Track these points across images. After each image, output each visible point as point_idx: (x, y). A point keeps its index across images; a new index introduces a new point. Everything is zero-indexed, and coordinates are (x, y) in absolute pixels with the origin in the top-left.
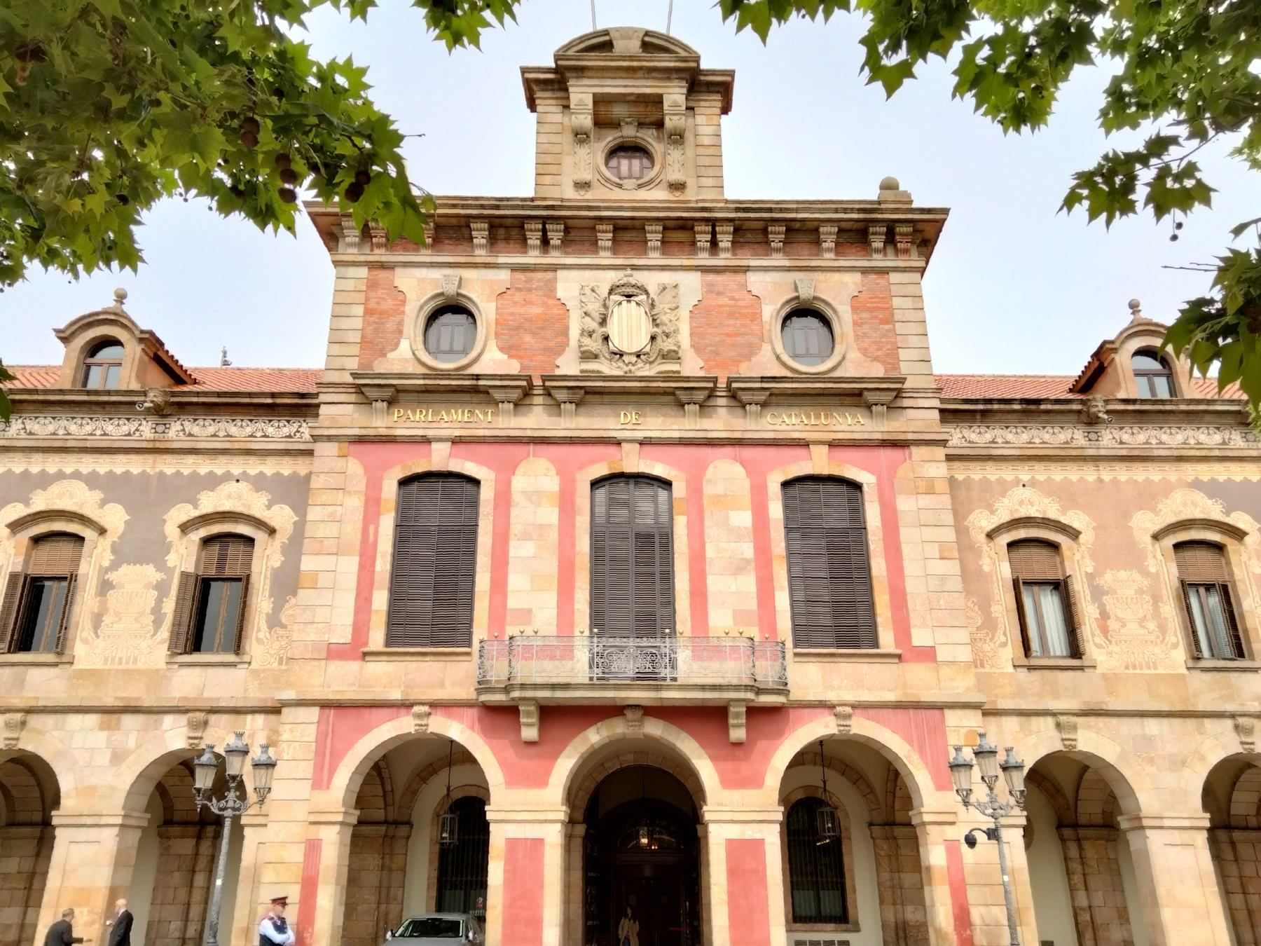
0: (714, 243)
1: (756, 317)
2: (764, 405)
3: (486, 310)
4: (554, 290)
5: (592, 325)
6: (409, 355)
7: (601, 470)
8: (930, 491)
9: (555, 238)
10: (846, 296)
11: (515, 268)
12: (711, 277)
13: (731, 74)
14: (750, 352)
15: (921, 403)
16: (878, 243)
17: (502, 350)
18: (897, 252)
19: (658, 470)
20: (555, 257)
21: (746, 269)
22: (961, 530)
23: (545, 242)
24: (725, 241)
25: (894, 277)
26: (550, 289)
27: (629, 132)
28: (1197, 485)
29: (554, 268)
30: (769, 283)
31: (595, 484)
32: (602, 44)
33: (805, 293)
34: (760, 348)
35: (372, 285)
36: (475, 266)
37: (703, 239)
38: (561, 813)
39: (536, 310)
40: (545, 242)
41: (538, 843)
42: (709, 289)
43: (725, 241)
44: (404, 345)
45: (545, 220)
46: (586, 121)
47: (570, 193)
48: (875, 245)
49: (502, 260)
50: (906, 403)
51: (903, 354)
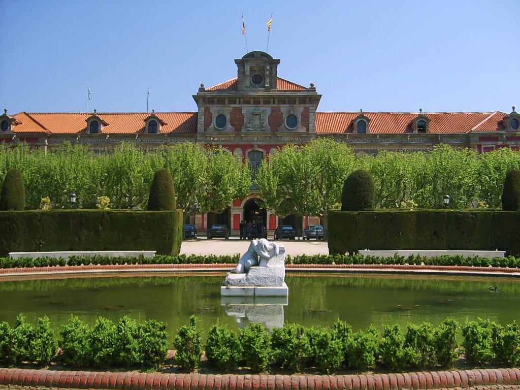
0: (274, 101)
3: (228, 117)
4: (241, 111)
6: (213, 126)
7: (250, 150)
9: (242, 100)
10: (300, 113)
11: (233, 108)
13: (280, 60)
14: (280, 125)
17: (231, 125)
18: (311, 103)
19: (261, 150)
20: (243, 105)
23: (240, 101)
24: (276, 100)
27: (257, 73)
30: (284, 108)
31: (249, 152)
32: (251, 55)
33: (292, 113)
34: (282, 124)
35: (205, 111)
36: (225, 107)
38: (243, 210)
39: (238, 116)
40: (240, 101)
41: (239, 215)
42: (273, 111)
43: (276, 100)
44: (212, 124)
46: (248, 73)
47: (245, 89)
49: (231, 105)
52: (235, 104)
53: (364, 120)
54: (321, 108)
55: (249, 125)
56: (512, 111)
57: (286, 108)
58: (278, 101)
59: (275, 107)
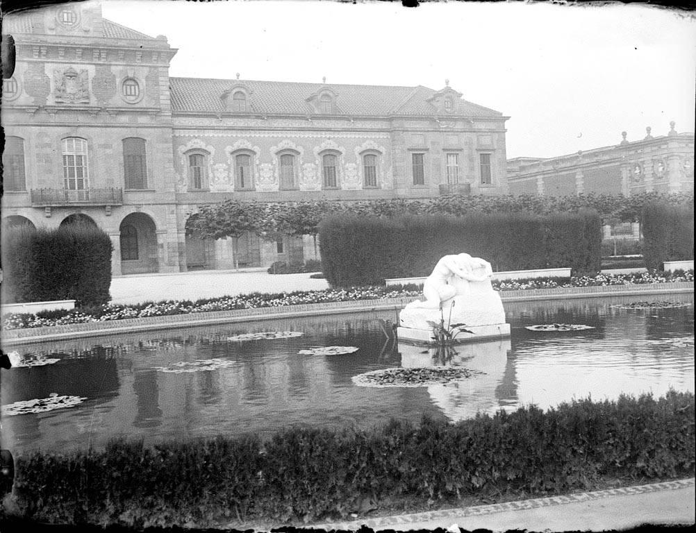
1: (114, 81)
2: (116, 114)
5: (59, 84)
8: (166, 142)
9: (44, 52)
11: (29, 62)
12: (99, 67)
15: (165, 114)
16: (154, 58)
20: (43, 59)
21: (110, 65)
22: (175, 152)
23: (40, 52)
24: (103, 55)
25: (160, 69)
26: (43, 71)
28: (247, 139)
29: (43, 62)
30: (118, 68)
33: (131, 75)
37: (96, 55)
40: (40, 52)
45: (40, 47)
47: (49, 32)
48: (154, 59)
50: (163, 114)
51: (162, 97)
52: (32, 57)
53: (243, 91)
54: (177, 68)
55: (58, 94)
56: (446, 86)
57: (121, 68)
58: (108, 54)
59: (100, 65)
